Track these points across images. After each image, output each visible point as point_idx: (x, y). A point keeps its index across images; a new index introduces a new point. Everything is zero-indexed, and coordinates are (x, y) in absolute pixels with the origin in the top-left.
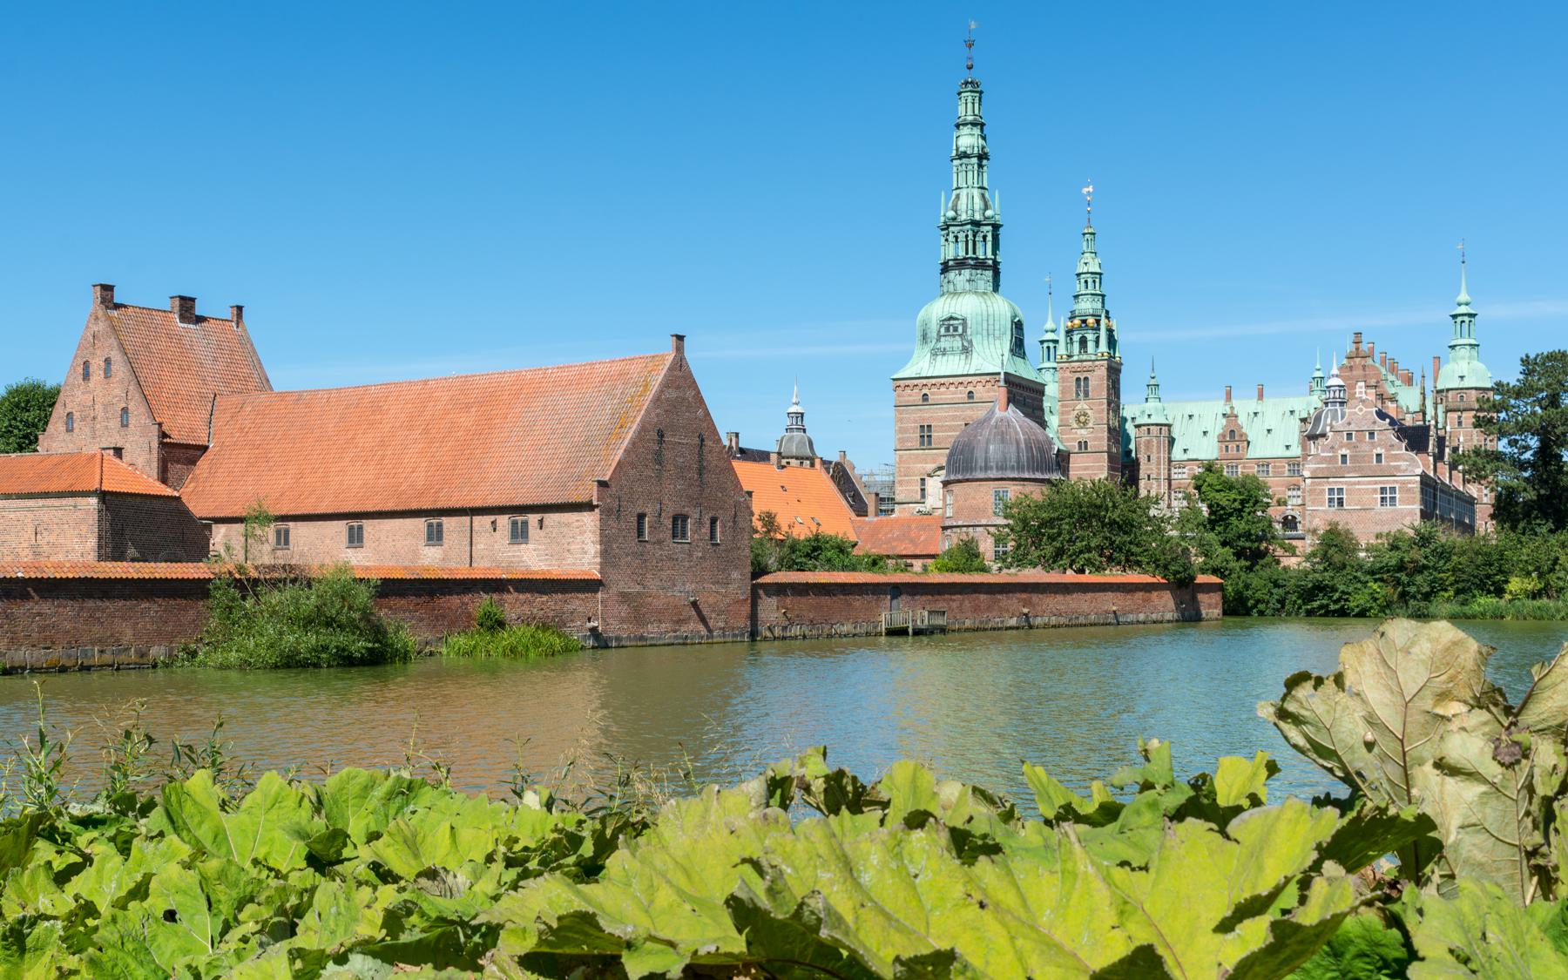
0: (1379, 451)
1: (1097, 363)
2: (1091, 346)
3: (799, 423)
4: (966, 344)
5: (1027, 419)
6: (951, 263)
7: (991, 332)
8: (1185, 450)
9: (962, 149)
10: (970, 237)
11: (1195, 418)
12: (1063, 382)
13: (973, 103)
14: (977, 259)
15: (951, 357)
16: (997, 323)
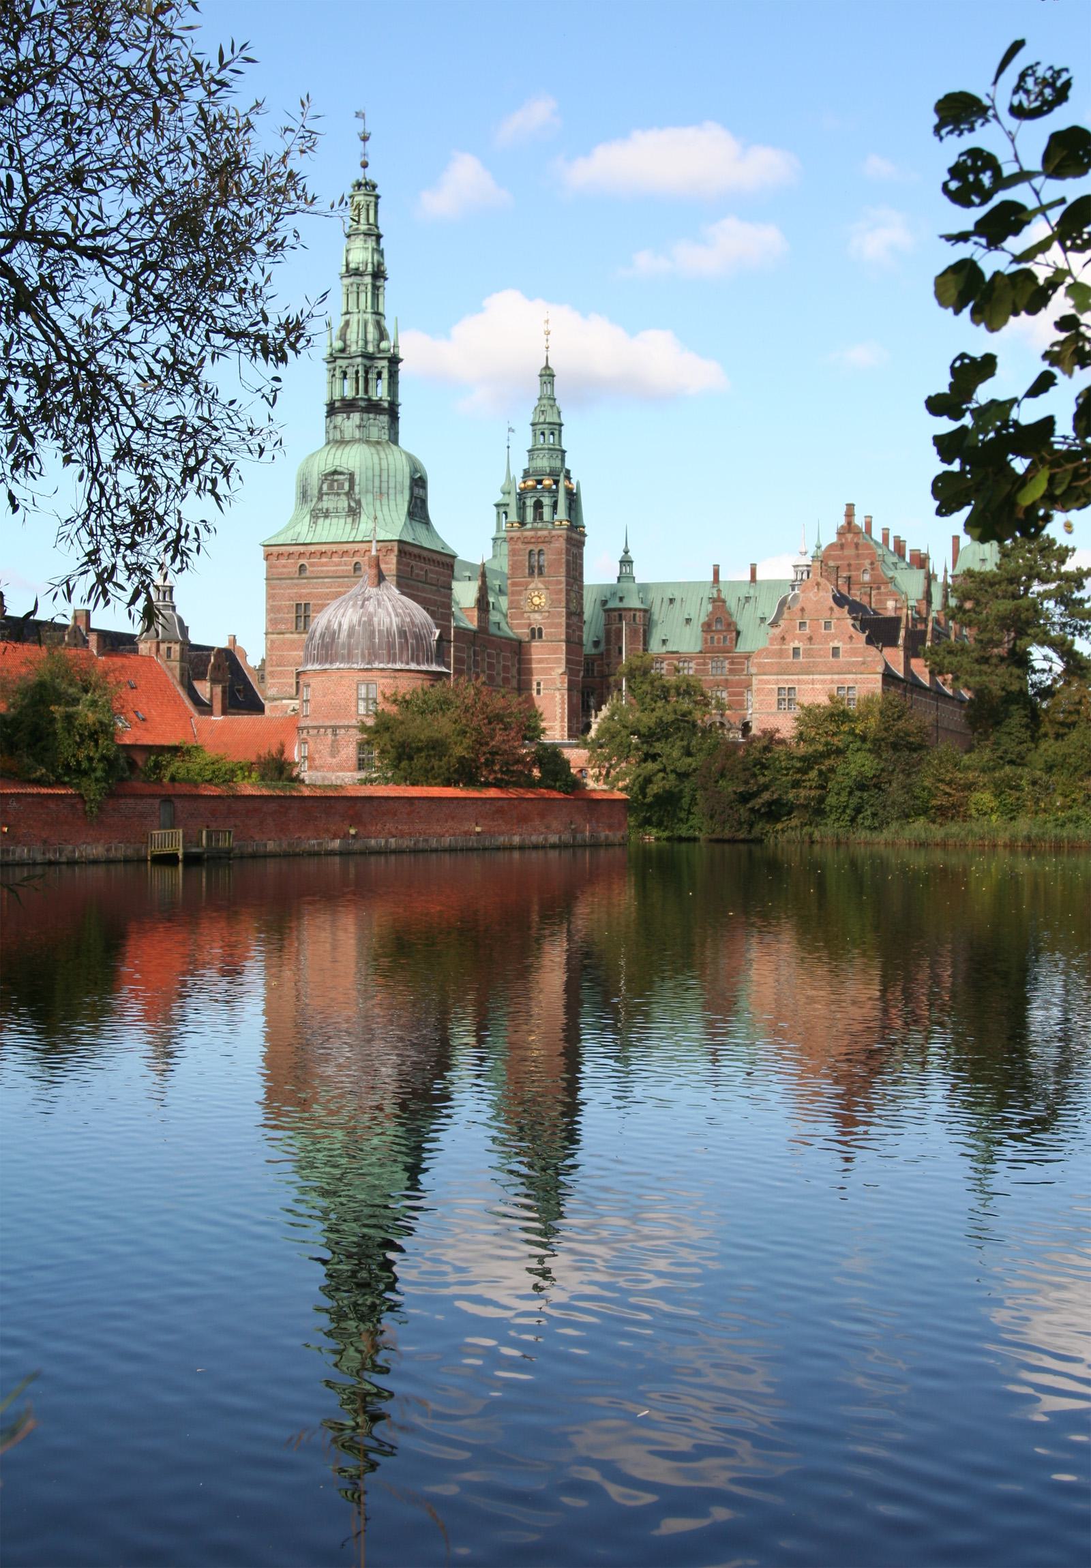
0: (836, 644)
1: (554, 533)
2: (547, 512)
3: (167, 599)
4: (353, 504)
5: (404, 598)
6: (337, 404)
7: (384, 490)
8: (664, 642)
9: (352, 266)
10: (361, 374)
11: (678, 602)
12: (514, 555)
13: (368, 210)
14: (369, 400)
15: (335, 521)
16: (392, 480)
